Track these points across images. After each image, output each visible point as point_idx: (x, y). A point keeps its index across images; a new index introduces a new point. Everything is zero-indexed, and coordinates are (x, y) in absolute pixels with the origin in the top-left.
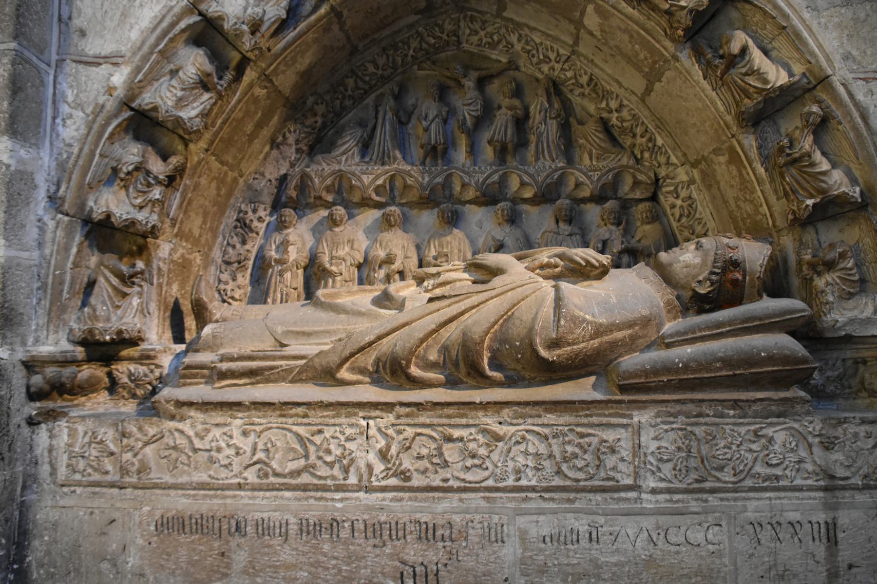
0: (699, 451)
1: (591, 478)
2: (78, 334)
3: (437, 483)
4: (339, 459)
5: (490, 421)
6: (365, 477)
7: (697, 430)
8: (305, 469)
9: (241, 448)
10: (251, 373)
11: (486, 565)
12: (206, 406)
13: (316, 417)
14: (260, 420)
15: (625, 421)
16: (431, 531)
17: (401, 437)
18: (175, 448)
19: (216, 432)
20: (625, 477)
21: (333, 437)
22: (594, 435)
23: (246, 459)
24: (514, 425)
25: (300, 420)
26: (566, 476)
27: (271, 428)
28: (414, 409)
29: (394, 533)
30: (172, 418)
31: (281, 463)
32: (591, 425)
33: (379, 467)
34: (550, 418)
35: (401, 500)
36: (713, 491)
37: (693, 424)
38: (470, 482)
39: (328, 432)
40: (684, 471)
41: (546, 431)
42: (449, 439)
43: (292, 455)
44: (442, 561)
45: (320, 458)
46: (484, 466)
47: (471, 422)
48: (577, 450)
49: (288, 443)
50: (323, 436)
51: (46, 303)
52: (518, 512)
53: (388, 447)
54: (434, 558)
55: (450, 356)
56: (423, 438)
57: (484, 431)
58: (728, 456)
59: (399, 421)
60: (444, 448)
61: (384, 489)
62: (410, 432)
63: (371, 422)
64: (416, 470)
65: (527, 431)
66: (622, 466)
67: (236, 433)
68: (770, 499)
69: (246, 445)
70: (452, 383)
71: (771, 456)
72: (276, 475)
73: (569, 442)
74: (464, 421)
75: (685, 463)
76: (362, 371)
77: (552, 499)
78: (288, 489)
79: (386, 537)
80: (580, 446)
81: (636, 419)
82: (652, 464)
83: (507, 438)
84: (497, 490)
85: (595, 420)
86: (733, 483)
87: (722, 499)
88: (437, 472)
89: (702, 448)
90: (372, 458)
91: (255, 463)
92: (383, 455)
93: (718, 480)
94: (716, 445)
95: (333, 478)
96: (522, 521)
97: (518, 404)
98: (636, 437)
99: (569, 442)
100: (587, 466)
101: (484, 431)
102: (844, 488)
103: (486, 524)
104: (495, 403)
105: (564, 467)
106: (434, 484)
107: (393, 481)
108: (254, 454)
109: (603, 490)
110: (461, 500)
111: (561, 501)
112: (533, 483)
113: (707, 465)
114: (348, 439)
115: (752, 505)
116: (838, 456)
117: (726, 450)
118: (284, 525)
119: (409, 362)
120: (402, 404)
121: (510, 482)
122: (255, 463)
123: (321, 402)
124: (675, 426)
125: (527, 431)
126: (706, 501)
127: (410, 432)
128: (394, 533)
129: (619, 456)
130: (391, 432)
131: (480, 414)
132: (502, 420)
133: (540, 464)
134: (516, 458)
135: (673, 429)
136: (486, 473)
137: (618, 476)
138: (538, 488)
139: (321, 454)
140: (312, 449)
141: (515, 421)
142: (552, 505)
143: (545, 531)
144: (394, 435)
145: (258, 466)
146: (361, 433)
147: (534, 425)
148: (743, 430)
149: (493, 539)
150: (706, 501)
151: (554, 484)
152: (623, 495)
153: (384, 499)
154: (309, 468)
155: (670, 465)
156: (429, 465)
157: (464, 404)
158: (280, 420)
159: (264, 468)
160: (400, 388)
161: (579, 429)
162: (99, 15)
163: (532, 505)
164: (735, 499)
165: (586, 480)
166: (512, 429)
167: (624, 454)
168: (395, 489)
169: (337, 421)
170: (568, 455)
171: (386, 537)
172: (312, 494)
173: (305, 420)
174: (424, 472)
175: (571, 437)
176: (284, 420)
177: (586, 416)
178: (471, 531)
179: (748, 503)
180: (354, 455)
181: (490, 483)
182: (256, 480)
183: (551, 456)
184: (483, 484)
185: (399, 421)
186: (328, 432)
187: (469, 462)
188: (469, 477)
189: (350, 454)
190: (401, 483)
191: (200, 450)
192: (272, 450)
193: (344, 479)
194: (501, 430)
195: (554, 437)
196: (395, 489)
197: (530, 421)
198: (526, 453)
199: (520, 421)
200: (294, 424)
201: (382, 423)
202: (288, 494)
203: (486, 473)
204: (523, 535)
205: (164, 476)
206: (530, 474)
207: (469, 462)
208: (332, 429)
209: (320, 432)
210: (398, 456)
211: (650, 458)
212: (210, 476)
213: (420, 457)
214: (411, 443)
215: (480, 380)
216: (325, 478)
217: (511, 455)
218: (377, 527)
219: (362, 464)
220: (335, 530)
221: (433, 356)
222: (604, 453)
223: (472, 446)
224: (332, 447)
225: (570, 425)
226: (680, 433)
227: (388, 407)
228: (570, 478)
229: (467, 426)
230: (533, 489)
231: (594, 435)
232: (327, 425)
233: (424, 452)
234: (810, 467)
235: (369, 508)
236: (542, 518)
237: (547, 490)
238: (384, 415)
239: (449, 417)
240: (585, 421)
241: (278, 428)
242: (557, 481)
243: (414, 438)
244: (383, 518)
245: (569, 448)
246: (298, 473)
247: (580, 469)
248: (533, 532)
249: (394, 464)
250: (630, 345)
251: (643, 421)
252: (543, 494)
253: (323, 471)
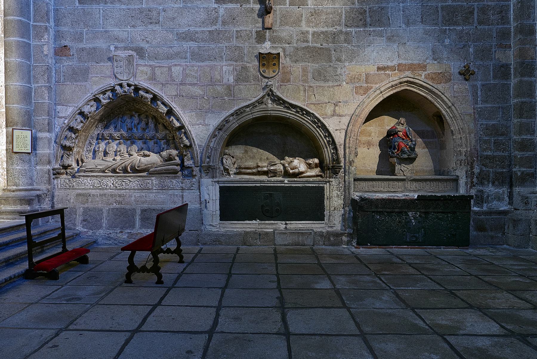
2: (61, 165)
5: (130, 179)
10: (91, 171)
12: (83, 176)
13: (102, 178)
14: (93, 178)
19: (86, 180)
30: (78, 178)
32: (145, 179)
33: (112, 186)
34: (139, 178)
42: (123, 181)
51: (55, 159)
61: (113, 189)
62: (117, 180)
67: (89, 180)
70: (124, 173)
76: (110, 171)
84: (131, 189)
85: (146, 179)
90: (111, 184)
92: (113, 184)
105: (141, 186)
107: (115, 188)
109: (147, 189)
115: (170, 192)
121: (133, 188)
127: (117, 180)
140: (101, 183)
148: (169, 180)
162: (61, 109)
168: (115, 189)
181: (130, 188)
183: (139, 184)
196: (115, 189)
213: (119, 184)
223: (127, 182)
230: (136, 189)
233: (119, 183)
235: (111, 192)
237: (138, 189)
242: (140, 188)
246: (99, 187)
248: (136, 196)
250: (152, 167)
253: (103, 186)
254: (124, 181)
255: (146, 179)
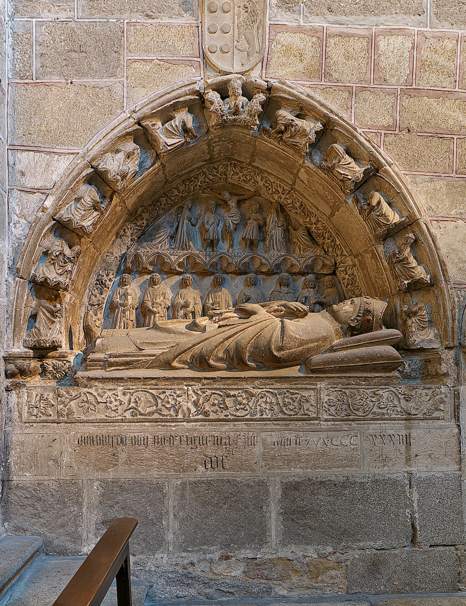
0: (348, 402)
1: (297, 414)
3: (223, 417)
4: (173, 406)
6: (187, 414)
7: (347, 391)
8: (156, 411)
9: (123, 401)
11: (246, 456)
13: (161, 385)
14: (133, 386)
15: (313, 387)
16: (219, 440)
17: (205, 395)
18: (87, 402)
20: (313, 413)
21: (170, 395)
22: (298, 394)
23: (125, 407)
24: (261, 389)
25: (153, 387)
26: (285, 413)
27: (138, 391)
28: (212, 381)
29: (201, 441)
31: (143, 408)
32: (297, 389)
33: (193, 410)
34: (278, 385)
35: (205, 425)
36: (354, 420)
37: (345, 389)
38: (239, 417)
39: (168, 393)
40: (340, 411)
41: (276, 392)
42: (229, 396)
43: (149, 405)
44: (225, 455)
45: (164, 406)
46: (246, 409)
47: (239, 387)
48: (290, 401)
49: (147, 398)
50: (165, 395)
52: (262, 431)
53: (198, 400)
54: (221, 453)
55: (229, 355)
56: (216, 395)
57: (246, 392)
58: (361, 404)
59: (204, 387)
60: (226, 400)
61: (196, 421)
62: (209, 392)
63: (190, 388)
64: (212, 411)
65: (267, 392)
66: (311, 408)
68: (380, 424)
69: (125, 399)
70: (229, 369)
71: (381, 404)
72: (141, 414)
73: (287, 397)
74: (236, 387)
75: (341, 407)
77: (278, 424)
78: (148, 422)
79: (197, 444)
80: (292, 399)
81: (318, 386)
82: (325, 407)
83: (257, 395)
84: (252, 420)
85: (299, 386)
86: (363, 416)
87: (358, 424)
88: (222, 412)
89: (350, 400)
90: (190, 405)
91: (130, 409)
92: (196, 404)
93: (357, 415)
94: (356, 398)
95: (171, 415)
96: (263, 435)
97: (263, 378)
98: (318, 395)
99: (287, 397)
100: (295, 408)
101: (246, 392)
102: (414, 419)
103: (246, 437)
104: (252, 378)
105: (284, 409)
106: (221, 418)
107: (200, 417)
108: (130, 404)
109: (303, 420)
110: (234, 425)
111: (282, 425)
112: (269, 416)
113: (352, 408)
114: (178, 396)
115: (372, 427)
116: (411, 404)
117: (360, 401)
118: (146, 439)
119: (209, 357)
120: (205, 378)
121: (258, 416)
122: (130, 409)
123: (165, 377)
124: (337, 389)
125: (267, 392)
126: (351, 425)
127: (209, 392)
128: (201, 441)
129: (310, 404)
130: (199, 392)
131: (244, 383)
132: (254, 386)
133: (272, 407)
134: (261, 405)
135: (336, 391)
136: (247, 412)
137: (310, 413)
138: (272, 419)
139: (164, 403)
140: (159, 401)
141: (260, 387)
142: (278, 427)
143: (275, 440)
144: (201, 394)
145: (131, 410)
146: (185, 393)
147: (270, 389)
149: (250, 444)
150: (351, 425)
151: (279, 417)
152: (312, 422)
153: (196, 425)
154: (158, 411)
155: (334, 408)
156: (218, 409)
157: (236, 378)
158: (143, 387)
159: (135, 411)
160: (204, 370)
161: (292, 391)
163: (269, 427)
164: (364, 424)
165: (294, 415)
166: (260, 391)
167: (312, 402)
168: (201, 420)
169: (172, 387)
170: (286, 403)
171: (197, 444)
172: (160, 423)
173: (156, 387)
174: (216, 412)
175: (288, 394)
176: (145, 387)
177: (295, 384)
178: (239, 440)
179: (370, 426)
180: (181, 404)
181: (248, 417)
182: (131, 417)
183: (278, 404)
184: (245, 417)
185: (204, 387)
186: (168, 393)
187: (238, 407)
188: (238, 414)
189: (179, 403)
190: (205, 418)
191: (101, 402)
192: (139, 402)
193: (176, 416)
194: (254, 391)
195: (280, 395)
196: (201, 420)
197: (268, 387)
198: (266, 402)
199: (263, 387)
200: (150, 389)
201: (195, 388)
202: (147, 424)
203: (247, 412)
204: (264, 442)
205: (81, 416)
206: (268, 413)
207: (238, 407)
208: (170, 391)
209: (164, 392)
210: (203, 403)
211: (325, 404)
212: (106, 416)
213: (214, 405)
214: (210, 398)
215: (244, 366)
216: (167, 416)
217: (259, 403)
218: (193, 439)
219: (185, 408)
220: (172, 441)
221: (221, 355)
222: (303, 402)
223: (240, 399)
224: (170, 400)
225: (287, 389)
226: (339, 392)
227: (199, 379)
228: (287, 414)
229: (238, 389)
230: (269, 420)
231: (298, 394)
232: (168, 389)
233: (216, 402)
234: (399, 409)
235: (189, 430)
236: (273, 433)
238: (196, 384)
239: (228, 385)
240: (294, 386)
241: (142, 391)
242: (281, 416)
243: (211, 395)
244: (196, 435)
245: (286, 400)
247: (291, 410)
248: (269, 440)
249: (201, 408)
251: (322, 387)
252: (274, 422)
253: (165, 412)
254: (232, 393)
255: (299, 386)
